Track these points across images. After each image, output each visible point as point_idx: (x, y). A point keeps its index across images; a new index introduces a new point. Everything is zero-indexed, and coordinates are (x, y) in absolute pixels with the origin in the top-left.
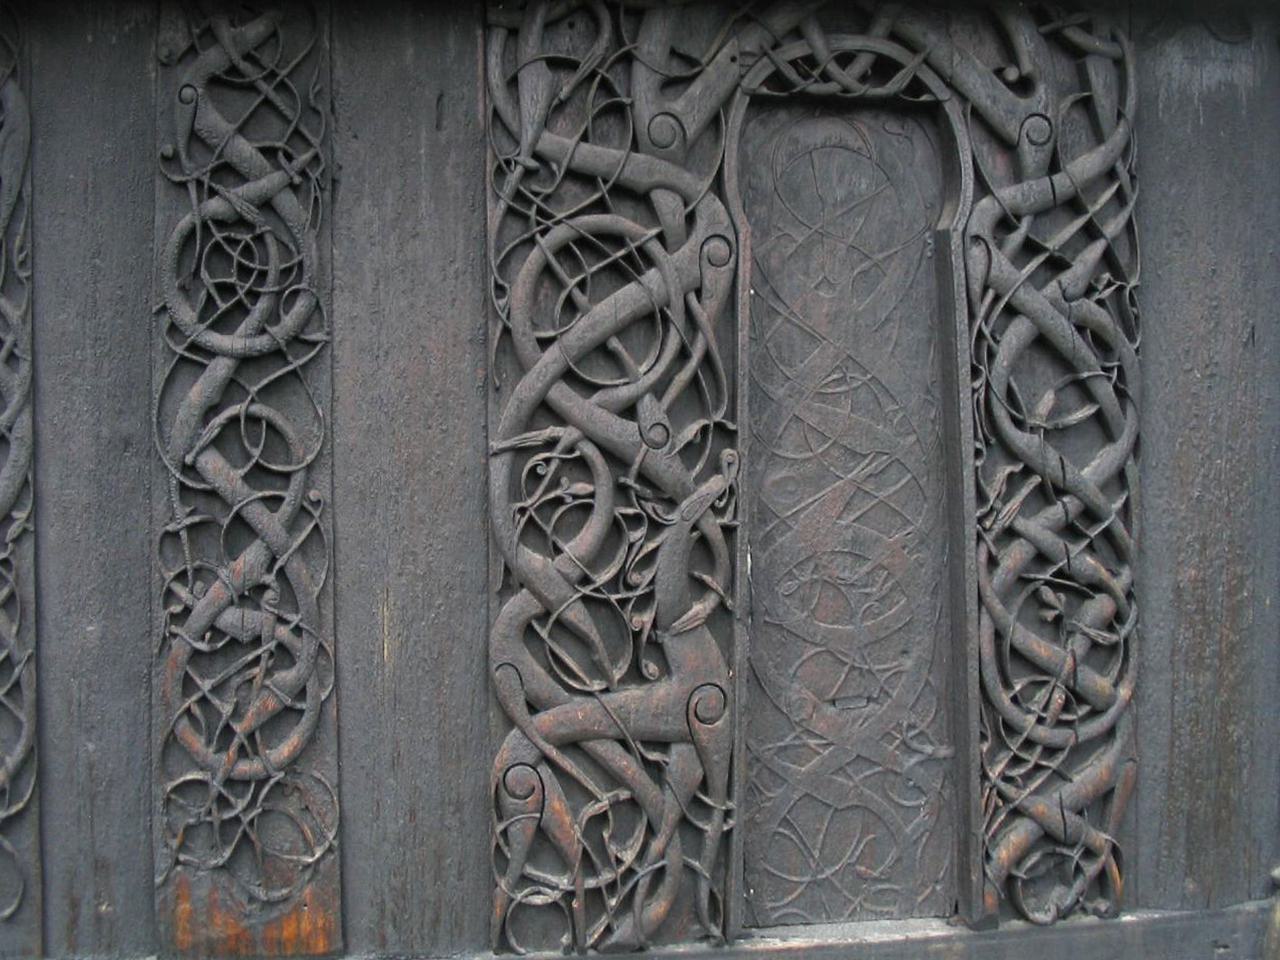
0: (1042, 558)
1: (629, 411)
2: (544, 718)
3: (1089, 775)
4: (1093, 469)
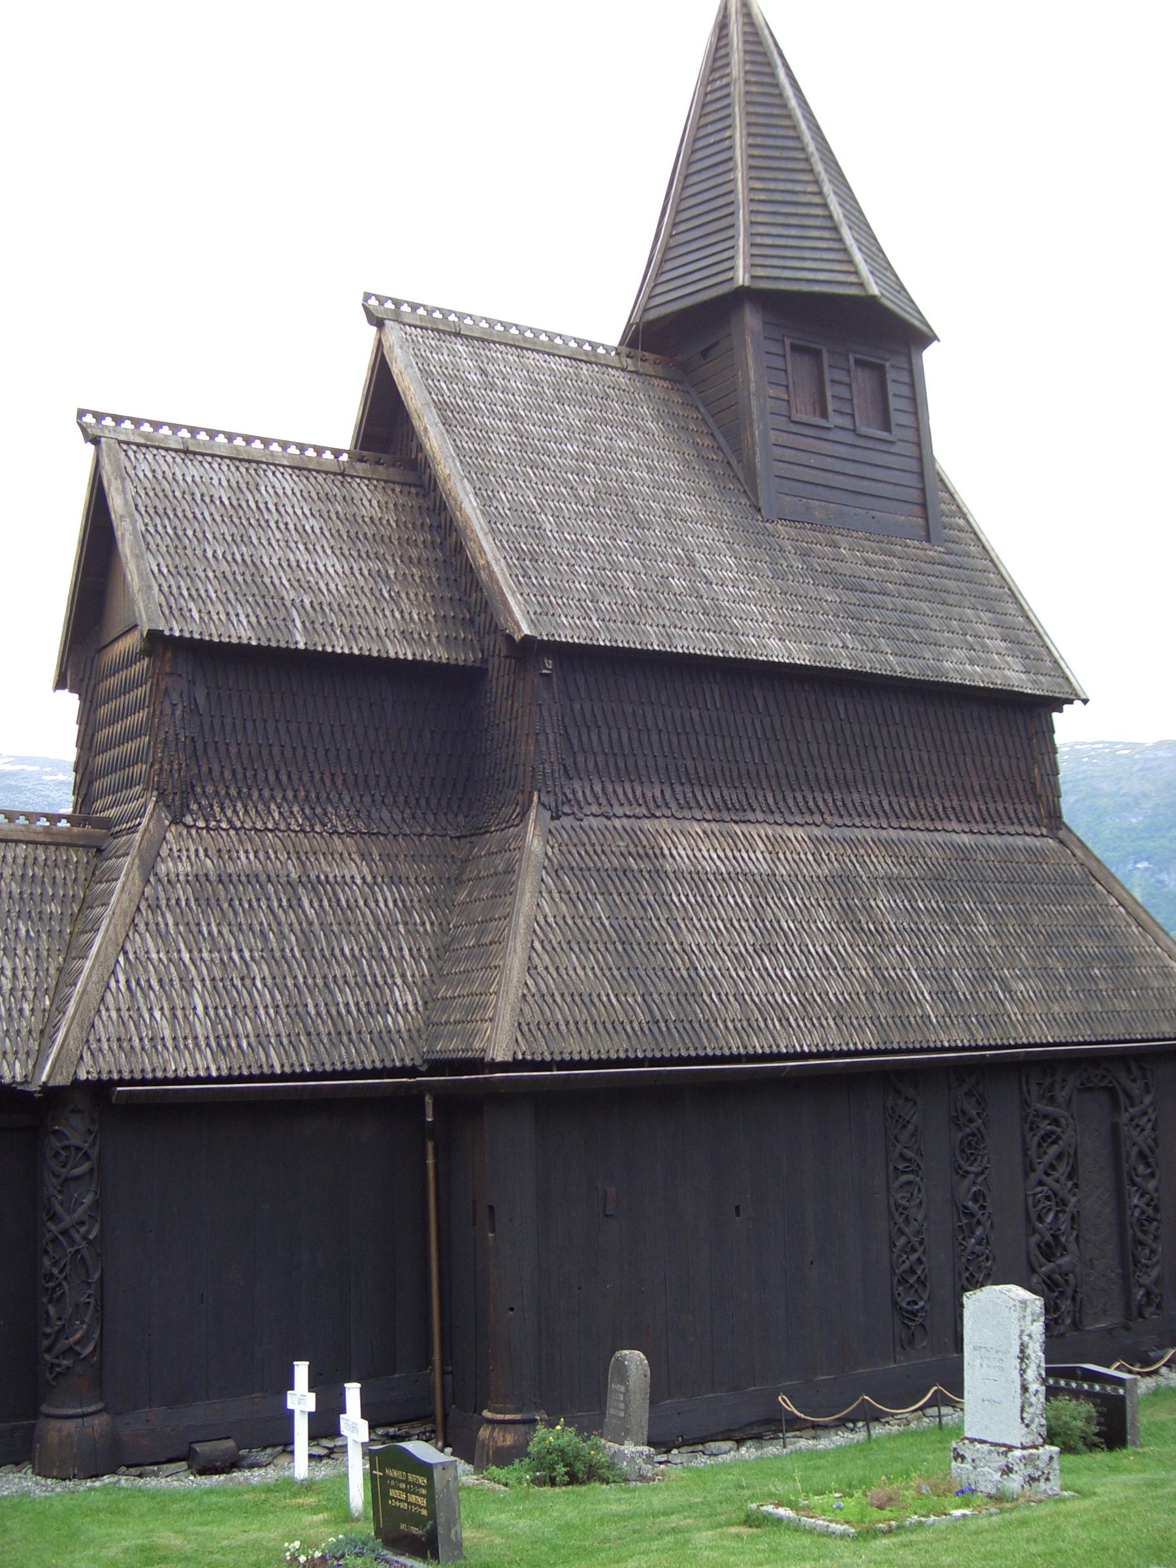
0: (1143, 1213)
1: (1057, 1181)
2: (1043, 1269)
3: (1154, 1273)
4: (1151, 1185)
